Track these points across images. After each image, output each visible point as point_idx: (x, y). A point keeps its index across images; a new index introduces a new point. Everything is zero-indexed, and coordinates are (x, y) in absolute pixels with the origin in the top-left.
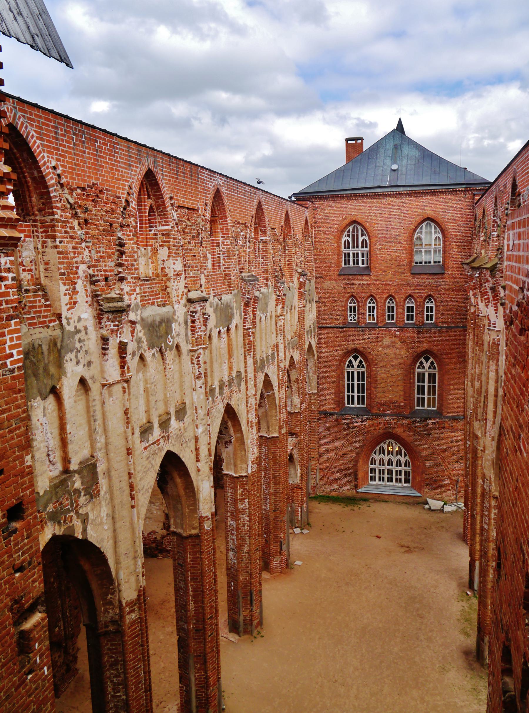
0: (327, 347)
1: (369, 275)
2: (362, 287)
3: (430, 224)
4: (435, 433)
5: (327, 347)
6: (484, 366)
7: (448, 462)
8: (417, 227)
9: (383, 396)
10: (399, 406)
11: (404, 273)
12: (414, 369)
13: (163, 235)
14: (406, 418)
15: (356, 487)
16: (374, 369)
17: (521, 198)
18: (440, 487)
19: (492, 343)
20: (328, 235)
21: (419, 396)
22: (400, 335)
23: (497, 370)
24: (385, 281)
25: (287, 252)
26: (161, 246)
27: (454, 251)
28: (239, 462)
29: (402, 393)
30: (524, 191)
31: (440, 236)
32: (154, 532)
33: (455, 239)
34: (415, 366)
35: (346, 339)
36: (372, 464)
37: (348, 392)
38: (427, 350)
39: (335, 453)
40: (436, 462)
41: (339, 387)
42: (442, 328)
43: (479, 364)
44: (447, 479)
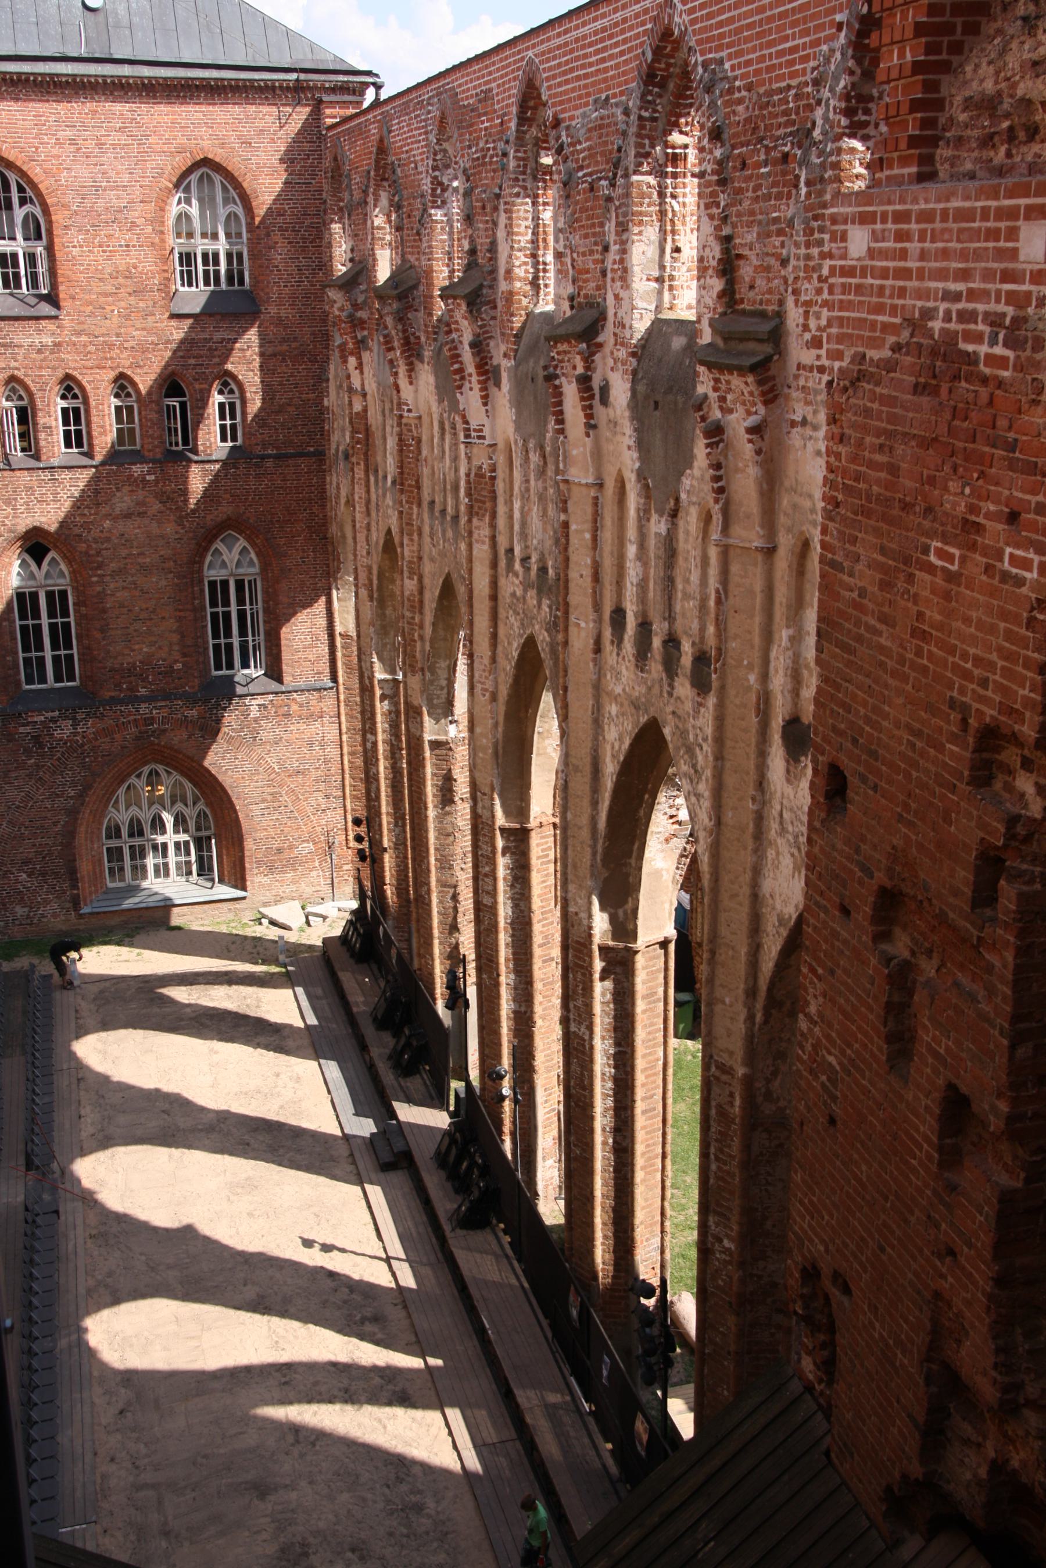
1: (56, 317)
2: (39, 351)
3: (208, 175)
4: (268, 731)
6: (427, 540)
7: (306, 799)
9: (126, 651)
10: (170, 671)
12: (200, 570)
14: (192, 700)
15: (76, 903)
16: (95, 579)
17: (564, 133)
18: (293, 864)
19: (476, 475)
21: (217, 641)
22: (157, 481)
23: (493, 538)
24: (103, 335)
27: (280, 254)
29: (175, 638)
30: (572, 118)
31: (240, 211)
33: (280, 220)
34: (201, 563)
36: (109, 837)
37: (26, 648)
38: (229, 519)
39: (10, 822)
40: (276, 804)
42: (263, 457)
43: (410, 534)
44: (307, 841)
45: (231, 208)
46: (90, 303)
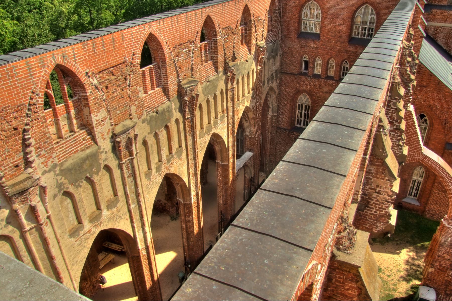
0: (286, 86)
2: (313, 48)
5: (286, 86)
8: (357, 9)
11: (343, 43)
13: (84, 99)
20: (292, 8)
25: (248, 32)
26: (84, 106)
28: (185, 196)
31: (375, 17)
32: (160, 200)
35: (299, 83)
41: (292, 113)
45: (373, 16)
46: (328, 38)
